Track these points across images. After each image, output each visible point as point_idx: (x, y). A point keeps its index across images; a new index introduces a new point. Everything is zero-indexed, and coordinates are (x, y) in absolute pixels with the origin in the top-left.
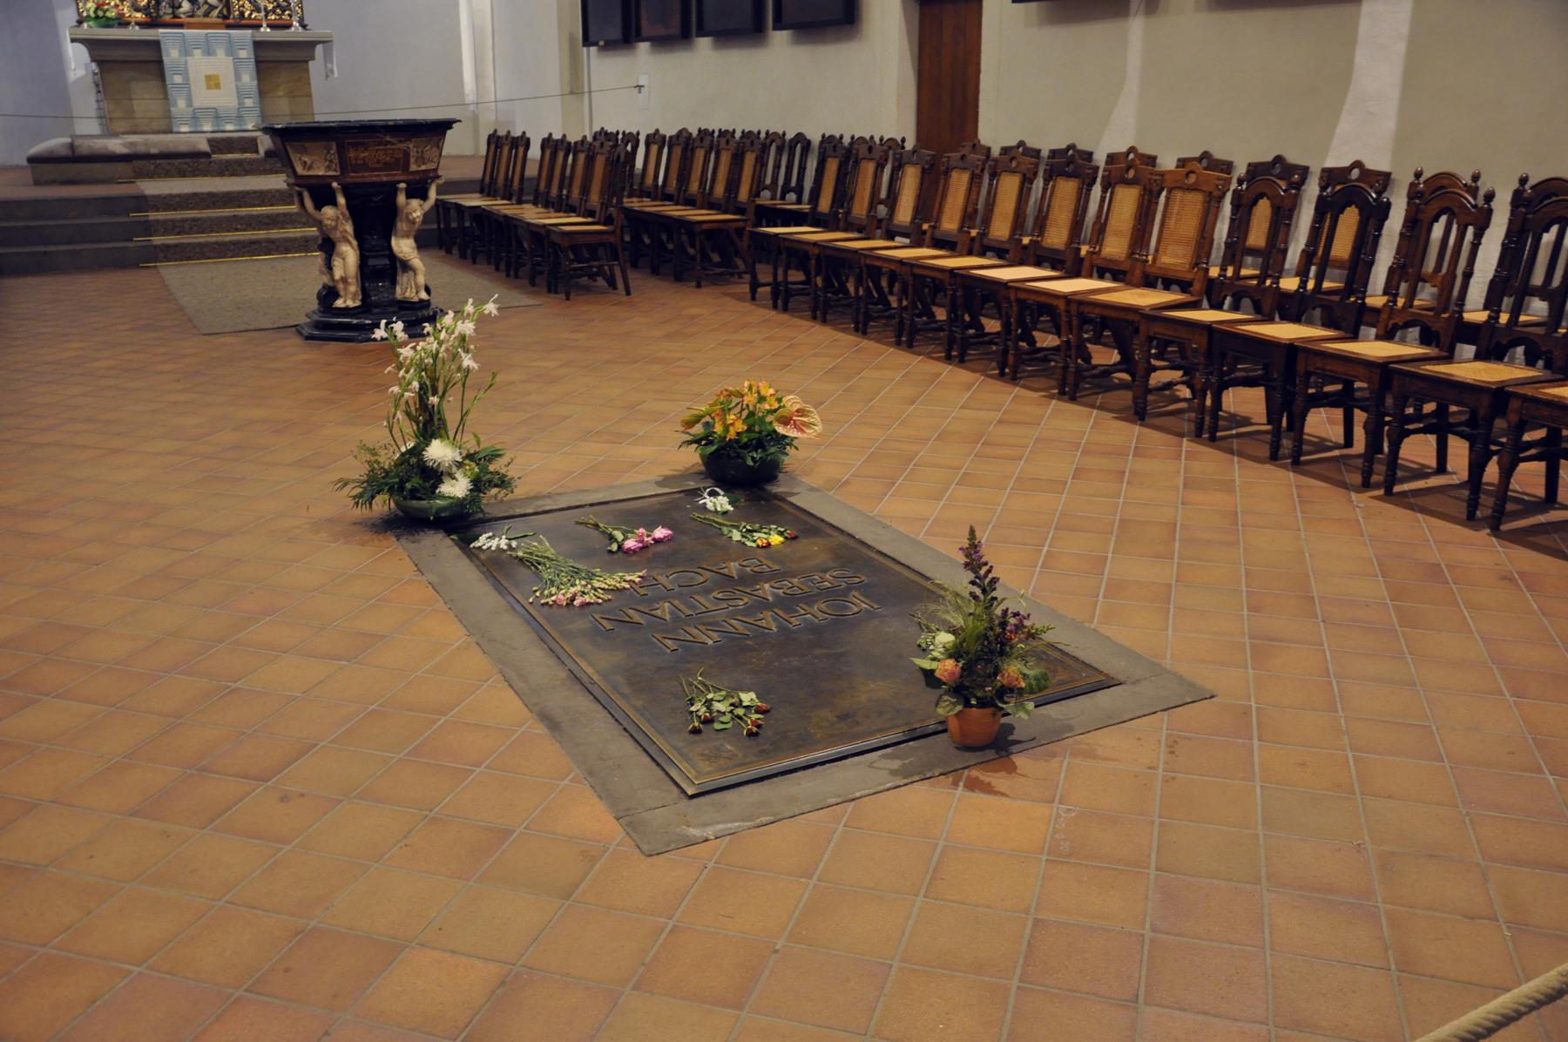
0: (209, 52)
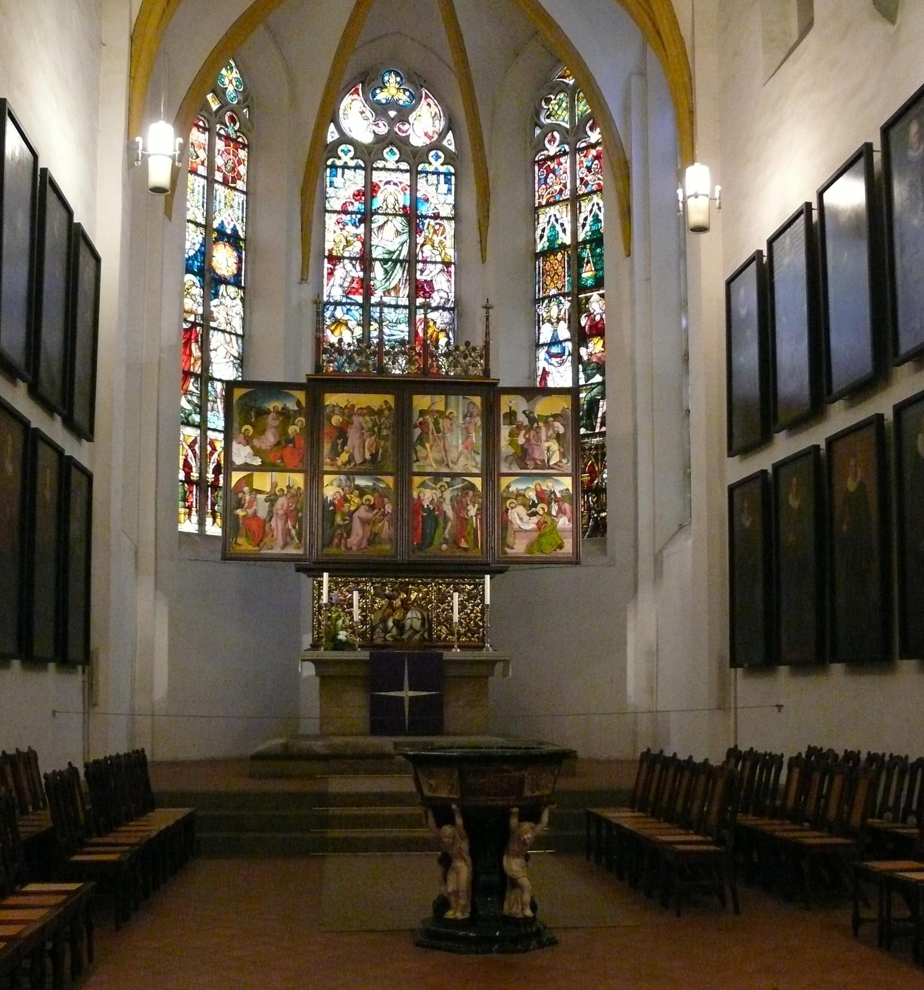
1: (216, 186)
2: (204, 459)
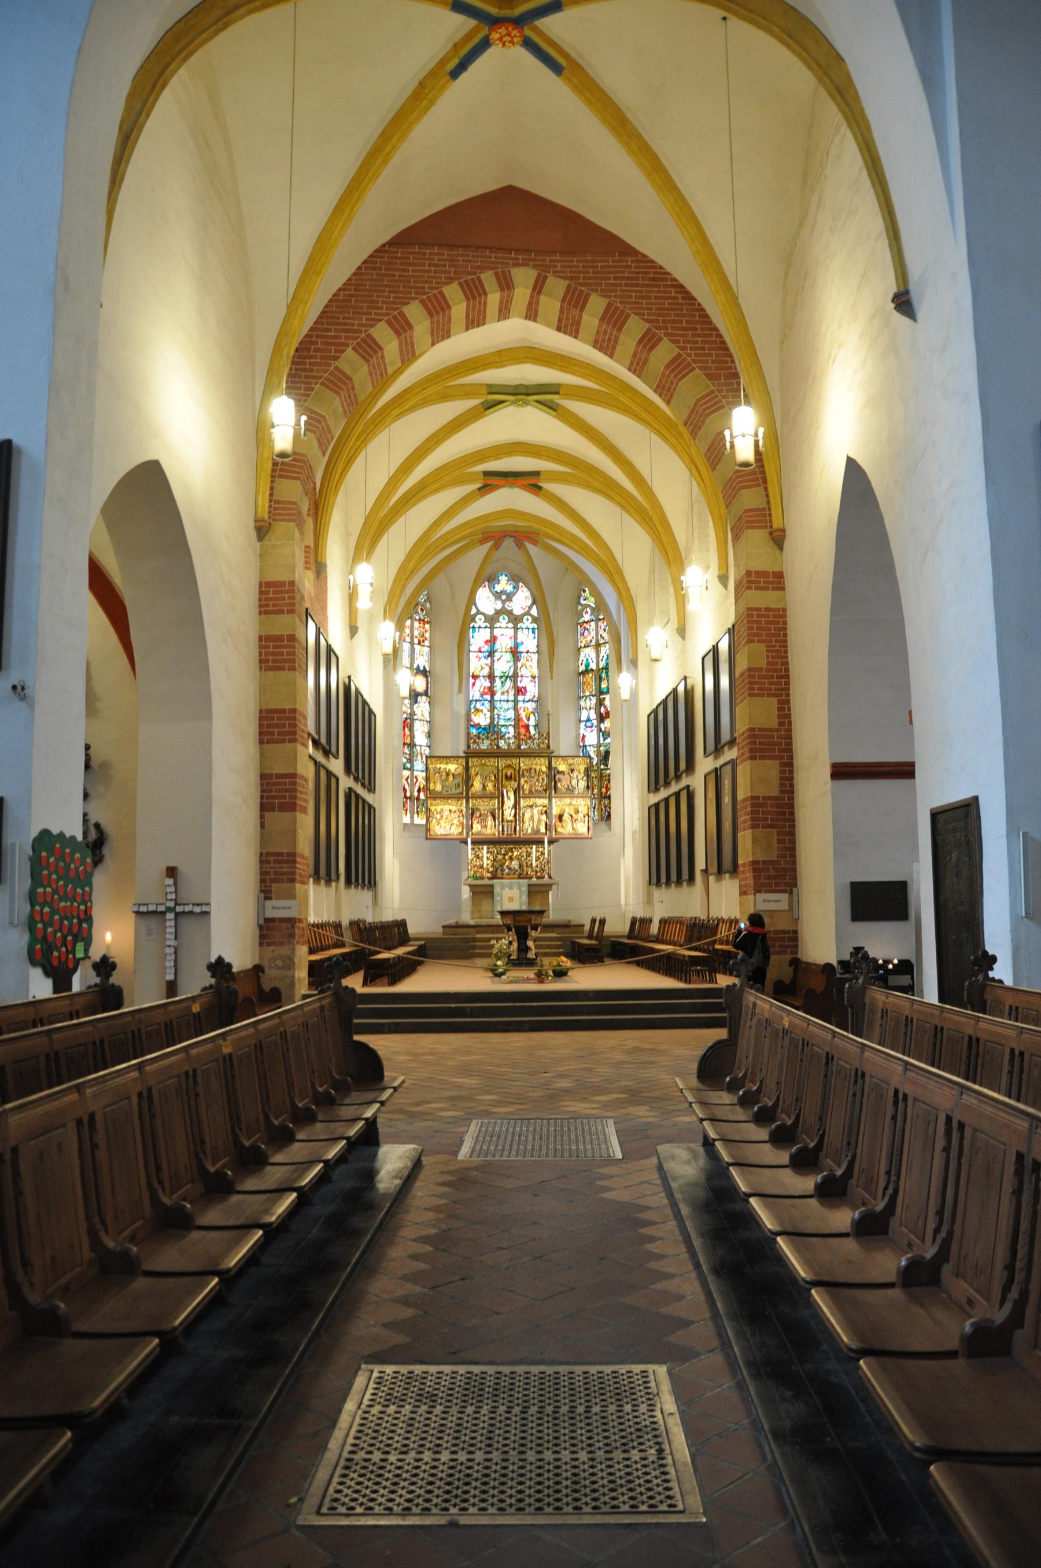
0: (511, 888)
1: (416, 646)
2: (412, 786)
